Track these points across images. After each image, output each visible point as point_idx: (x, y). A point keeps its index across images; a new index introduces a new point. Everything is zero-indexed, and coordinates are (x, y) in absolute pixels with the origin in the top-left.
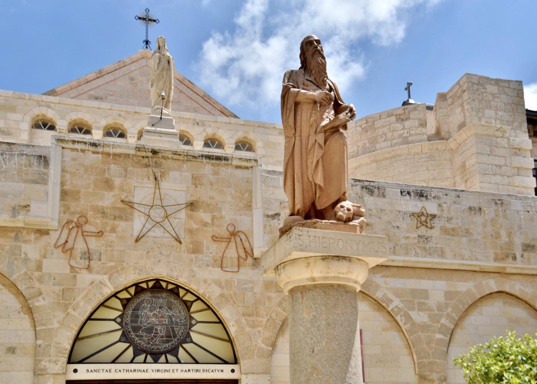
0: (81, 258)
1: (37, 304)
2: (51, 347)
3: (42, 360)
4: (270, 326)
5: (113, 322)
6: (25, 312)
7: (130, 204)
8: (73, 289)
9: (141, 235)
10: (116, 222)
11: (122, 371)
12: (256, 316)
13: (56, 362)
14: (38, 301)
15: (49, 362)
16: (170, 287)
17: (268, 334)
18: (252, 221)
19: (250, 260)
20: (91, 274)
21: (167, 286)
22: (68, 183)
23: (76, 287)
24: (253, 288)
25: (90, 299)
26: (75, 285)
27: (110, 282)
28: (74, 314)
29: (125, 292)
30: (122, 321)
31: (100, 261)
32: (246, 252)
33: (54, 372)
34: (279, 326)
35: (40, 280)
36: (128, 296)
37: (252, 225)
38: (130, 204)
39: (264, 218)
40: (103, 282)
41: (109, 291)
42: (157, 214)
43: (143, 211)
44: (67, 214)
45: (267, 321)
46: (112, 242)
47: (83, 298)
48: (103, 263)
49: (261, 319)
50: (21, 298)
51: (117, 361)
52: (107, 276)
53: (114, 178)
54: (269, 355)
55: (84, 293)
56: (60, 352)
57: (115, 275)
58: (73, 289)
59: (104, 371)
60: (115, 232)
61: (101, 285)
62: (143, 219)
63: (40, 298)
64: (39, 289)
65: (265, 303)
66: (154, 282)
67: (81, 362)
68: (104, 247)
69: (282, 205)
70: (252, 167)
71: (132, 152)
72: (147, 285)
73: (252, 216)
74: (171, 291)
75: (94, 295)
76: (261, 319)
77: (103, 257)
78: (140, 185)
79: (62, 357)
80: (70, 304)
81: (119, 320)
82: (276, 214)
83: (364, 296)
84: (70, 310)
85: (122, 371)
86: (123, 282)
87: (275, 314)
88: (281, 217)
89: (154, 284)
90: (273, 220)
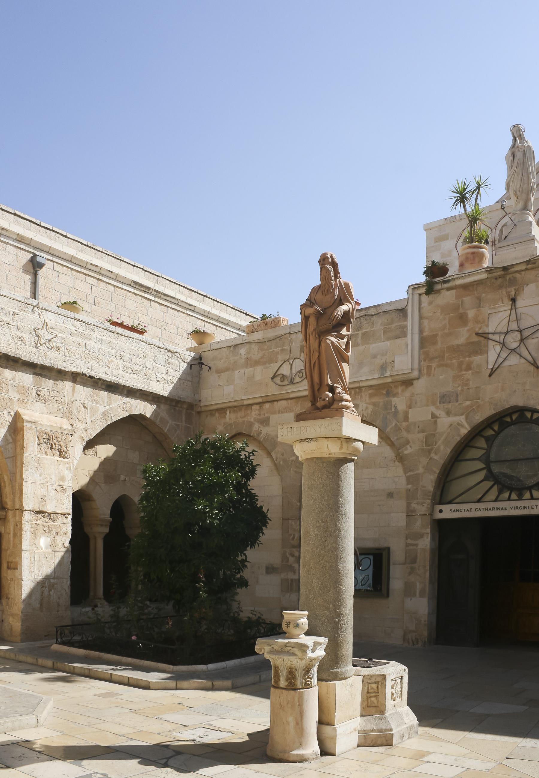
0: (440, 403)
1: (406, 452)
2: (418, 491)
6: (399, 461)
7: (485, 336)
9: (496, 366)
10: (471, 359)
11: (482, 510)
13: (422, 504)
20: (450, 416)
22: (426, 329)
23: (437, 432)
26: (436, 430)
27: (467, 422)
28: (436, 458)
31: (457, 402)
33: (422, 513)
35: (408, 430)
38: (484, 335)
40: (461, 423)
41: (464, 431)
42: (513, 341)
43: (498, 339)
44: (427, 361)
51: (482, 500)
52: (464, 417)
53: (468, 311)
59: (466, 510)
61: (459, 427)
62: (498, 348)
67: (450, 503)
71: (484, 276)
77: (459, 398)
78: (494, 311)
79: (428, 499)
85: (482, 510)
86: (479, 419)
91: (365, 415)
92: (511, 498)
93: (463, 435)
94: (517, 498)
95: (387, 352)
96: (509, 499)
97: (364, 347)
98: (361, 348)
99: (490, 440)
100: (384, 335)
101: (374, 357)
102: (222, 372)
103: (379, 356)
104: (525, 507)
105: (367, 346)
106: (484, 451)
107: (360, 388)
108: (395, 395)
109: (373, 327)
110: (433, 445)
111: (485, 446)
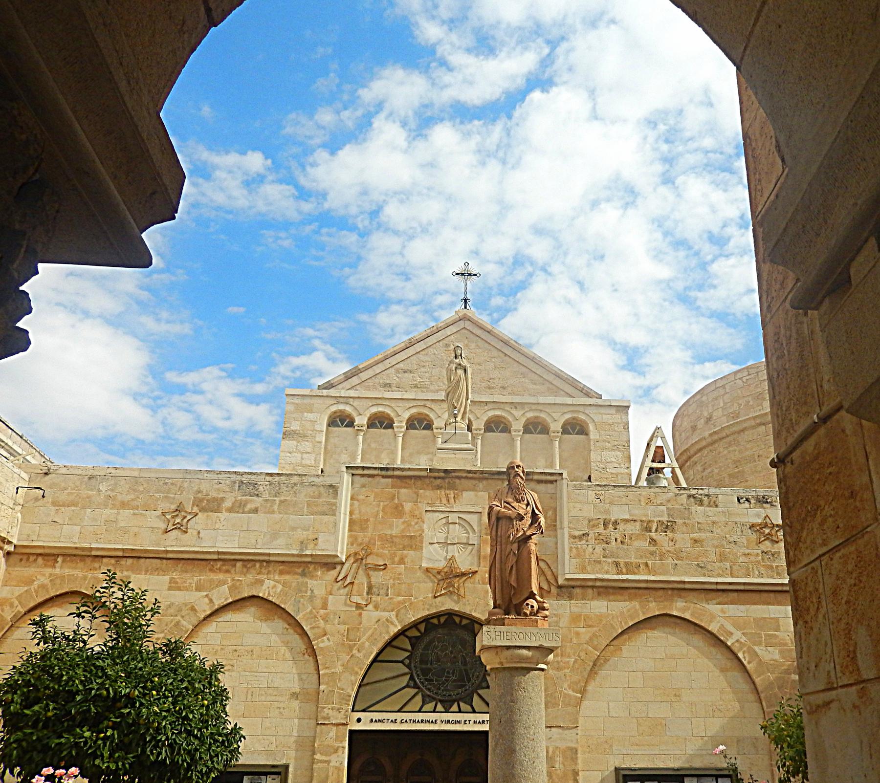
3: (325, 708)
4: (578, 669)
5: (400, 664)
8: (358, 629)
12: (562, 655)
14: (323, 641)
15: (332, 709)
16: (464, 622)
17: (576, 678)
18: (557, 543)
19: (554, 590)
21: (461, 622)
24: (557, 622)
25: (376, 639)
29: (414, 629)
30: (410, 662)
32: (549, 582)
34: (589, 669)
36: (419, 634)
37: (557, 548)
39: (569, 539)
41: (394, 630)
45: (574, 662)
46: (400, 574)
47: (368, 639)
48: (391, 599)
49: (568, 659)
50: (306, 639)
52: (394, 613)
54: (578, 703)
55: (370, 633)
56: (343, 699)
57: (403, 611)
58: (358, 629)
60: (404, 564)
63: (325, 638)
64: (324, 629)
65: (571, 639)
66: (446, 617)
68: (391, 581)
69: (591, 523)
70: (556, 481)
72: (439, 621)
73: (556, 537)
74: (465, 627)
75: (380, 635)
76: (568, 659)
80: (355, 645)
81: (407, 661)
82: (584, 535)
83: (697, 628)
84: (355, 652)
87: (584, 653)
88: (589, 537)
89: (446, 620)
90: (580, 541)
91: (271, 594)
92: (437, 710)
93: (392, 634)
94: (443, 710)
95: (309, 527)
96: (434, 711)
97: (281, 516)
98: (277, 516)
99: (414, 641)
100: (307, 508)
101: (294, 529)
102: (63, 506)
103: (299, 530)
104: (458, 722)
105: (285, 516)
106: (408, 654)
107: (268, 562)
108: (312, 577)
109: (295, 497)
110: (355, 641)
111: (410, 648)
